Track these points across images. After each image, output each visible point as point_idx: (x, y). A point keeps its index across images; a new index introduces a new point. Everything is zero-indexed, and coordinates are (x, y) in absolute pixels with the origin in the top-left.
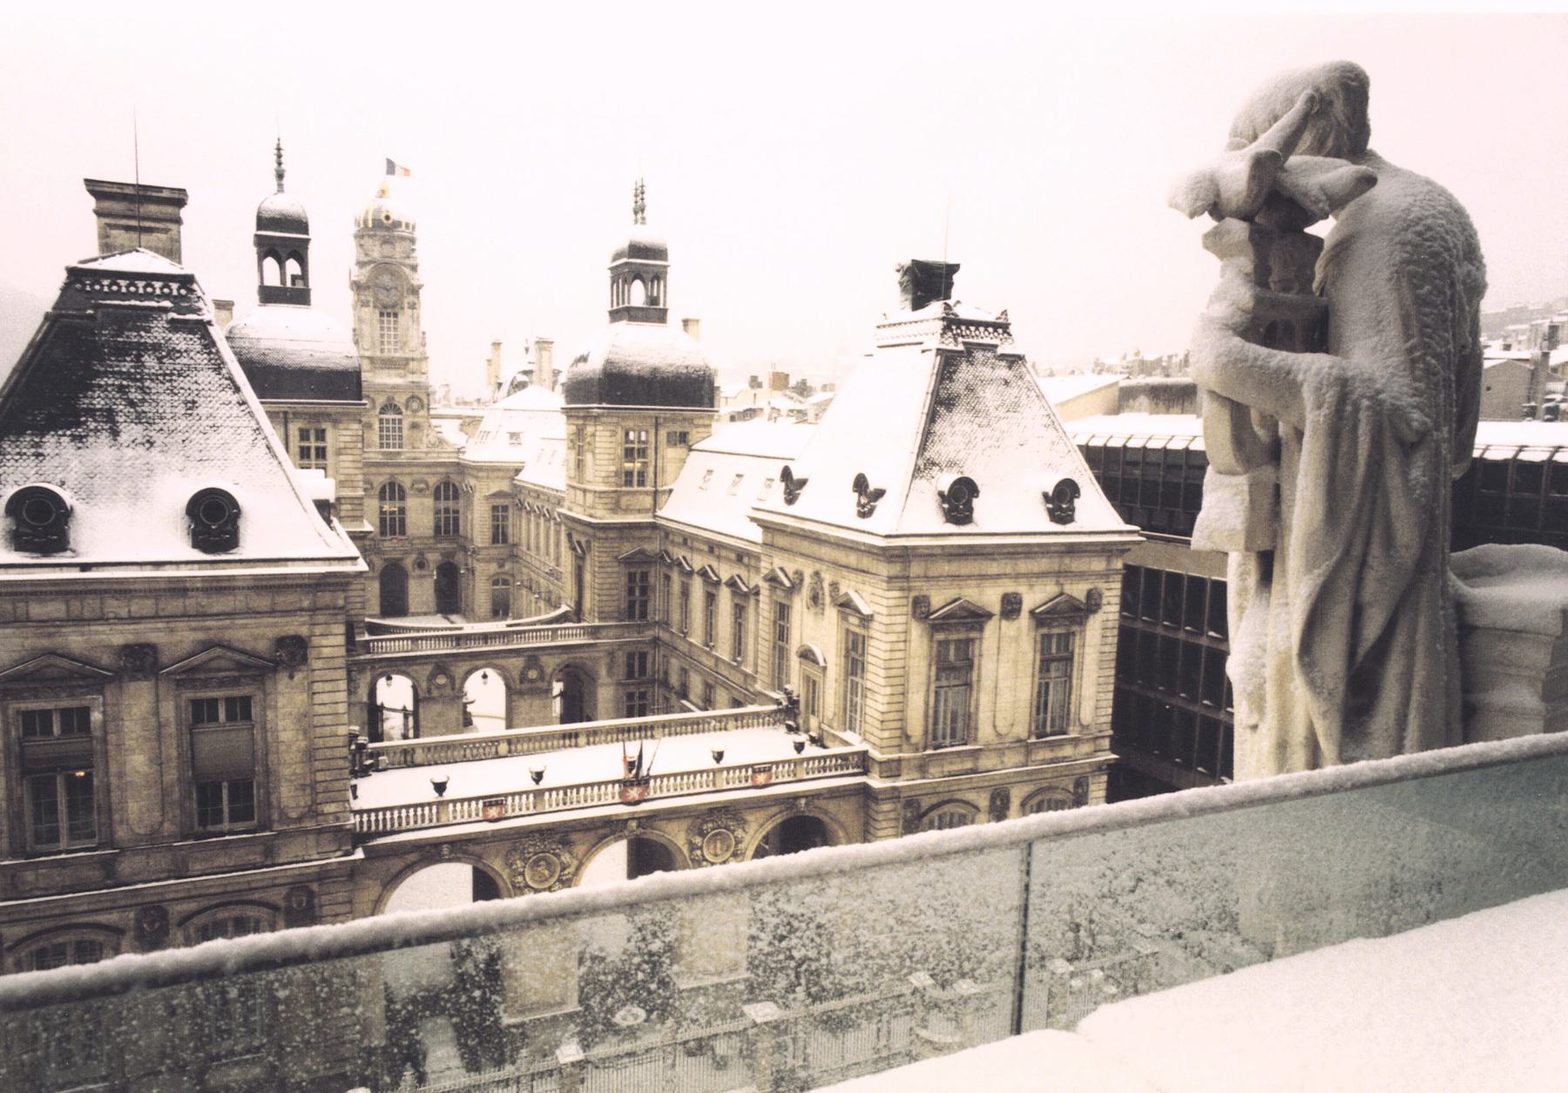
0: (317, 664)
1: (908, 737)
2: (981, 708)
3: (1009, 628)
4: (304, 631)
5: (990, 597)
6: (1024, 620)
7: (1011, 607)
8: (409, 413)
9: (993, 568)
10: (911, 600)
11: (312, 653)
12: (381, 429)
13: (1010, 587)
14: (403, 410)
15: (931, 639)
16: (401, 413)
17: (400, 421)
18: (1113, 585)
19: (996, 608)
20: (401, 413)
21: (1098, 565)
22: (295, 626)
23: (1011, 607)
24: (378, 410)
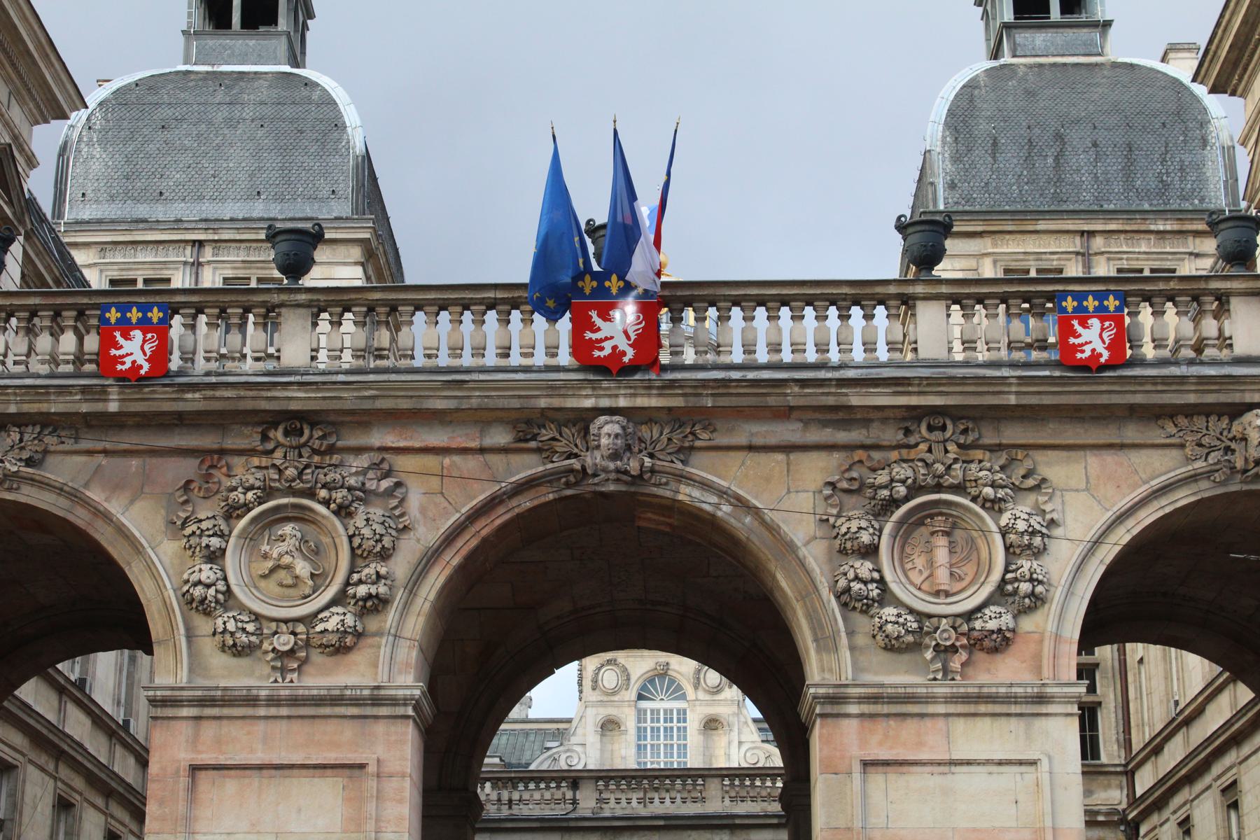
8: (701, 695)
12: (641, 733)
14: (689, 690)
16: (683, 697)
17: (682, 714)
20: (683, 697)
24: (634, 696)
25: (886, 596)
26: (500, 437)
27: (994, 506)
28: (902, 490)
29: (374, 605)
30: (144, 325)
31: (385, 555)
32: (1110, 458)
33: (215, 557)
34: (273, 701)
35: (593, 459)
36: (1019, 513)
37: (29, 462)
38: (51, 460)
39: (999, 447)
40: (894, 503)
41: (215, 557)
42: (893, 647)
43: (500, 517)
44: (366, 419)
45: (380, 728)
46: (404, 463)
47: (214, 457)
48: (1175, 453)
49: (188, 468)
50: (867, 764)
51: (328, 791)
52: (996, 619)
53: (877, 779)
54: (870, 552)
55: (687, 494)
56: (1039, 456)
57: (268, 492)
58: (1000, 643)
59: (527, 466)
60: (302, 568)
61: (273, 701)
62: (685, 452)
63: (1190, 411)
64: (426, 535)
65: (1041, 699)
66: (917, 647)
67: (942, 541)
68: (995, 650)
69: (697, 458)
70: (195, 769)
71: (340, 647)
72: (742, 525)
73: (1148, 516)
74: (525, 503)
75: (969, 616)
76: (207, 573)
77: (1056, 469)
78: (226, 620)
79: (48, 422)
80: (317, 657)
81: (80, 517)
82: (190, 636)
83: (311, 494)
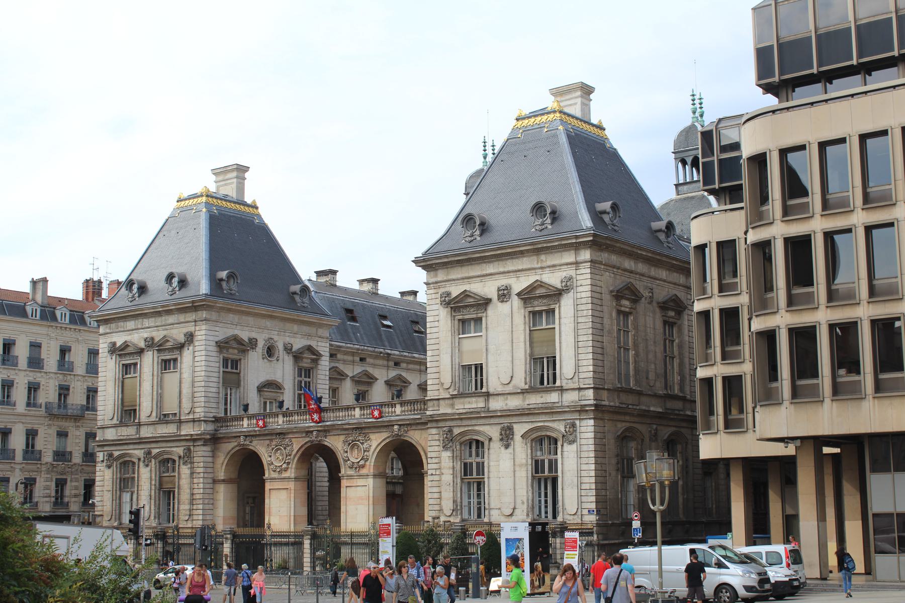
0: (197, 344)
1: (442, 384)
2: (489, 365)
3: (504, 308)
4: (192, 329)
5: (488, 289)
6: (516, 302)
7: (504, 294)
9: (490, 268)
10: (439, 294)
11: (196, 338)
13: (503, 281)
15: (453, 318)
18: (583, 271)
19: (494, 295)
21: (569, 257)
22: (190, 328)
23: (504, 294)
25: (349, 460)
26: (304, 435)
27: (362, 444)
28: (350, 442)
29: (288, 463)
30: (261, 419)
31: (290, 455)
32: (379, 434)
33: (270, 456)
34: (278, 479)
35: (314, 438)
36: (365, 445)
37: (250, 442)
38: (253, 442)
39: (364, 433)
40: (350, 444)
41: (270, 456)
42: (351, 468)
43: (304, 448)
44: (288, 433)
45: (290, 482)
46: (293, 440)
47: (271, 440)
48: (387, 433)
49: (268, 442)
50: (347, 487)
51: (285, 491)
52: (362, 463)
53: (348, 489)
54: (347, 452)
55: (326, 443)
56: (370, 434)
57: (277, 446)
58: (363, 466)
59: (307, 439)
60: (281, 458)
61: (278, 479)
62: (326, 437)
63: (386, 426)
64: (294, 453)
65: (368, 475)
66: (352, 468)
67: (356, 450)
68: (362, 468)
69: (328, 437)
70: (270, 489)
71: (286, 470)
72: (332, 448)
73: (383, 444)
74: (306, 446)
75: (358, 462)
76: (269, 459)
77: (372, 436)
78: (272, 467)
79: (252, 436)
80: (283, 472)
81: (256, 451)
82: (269, 469)
83: (281, 446)
